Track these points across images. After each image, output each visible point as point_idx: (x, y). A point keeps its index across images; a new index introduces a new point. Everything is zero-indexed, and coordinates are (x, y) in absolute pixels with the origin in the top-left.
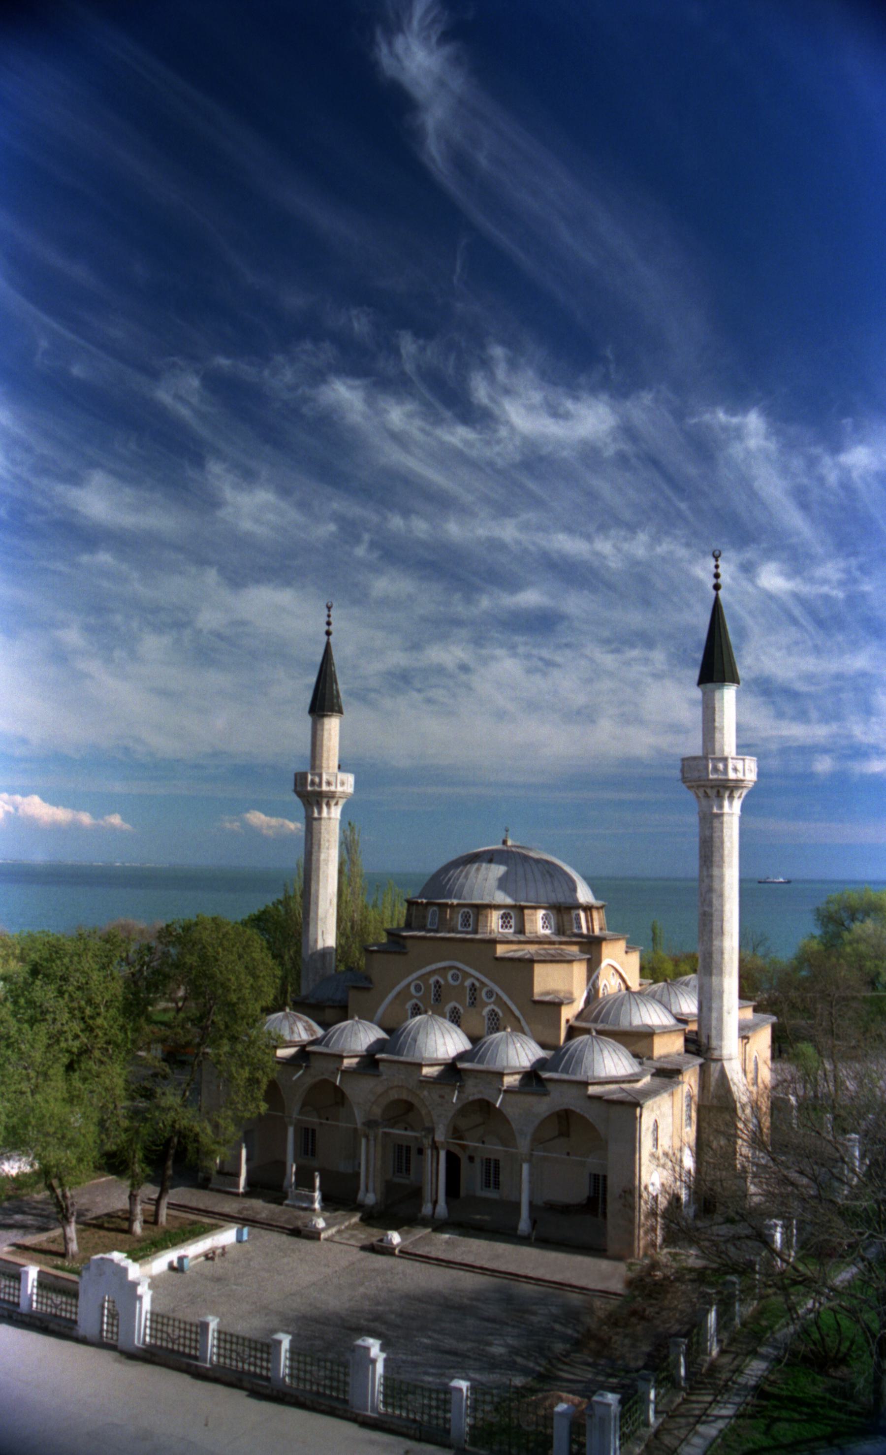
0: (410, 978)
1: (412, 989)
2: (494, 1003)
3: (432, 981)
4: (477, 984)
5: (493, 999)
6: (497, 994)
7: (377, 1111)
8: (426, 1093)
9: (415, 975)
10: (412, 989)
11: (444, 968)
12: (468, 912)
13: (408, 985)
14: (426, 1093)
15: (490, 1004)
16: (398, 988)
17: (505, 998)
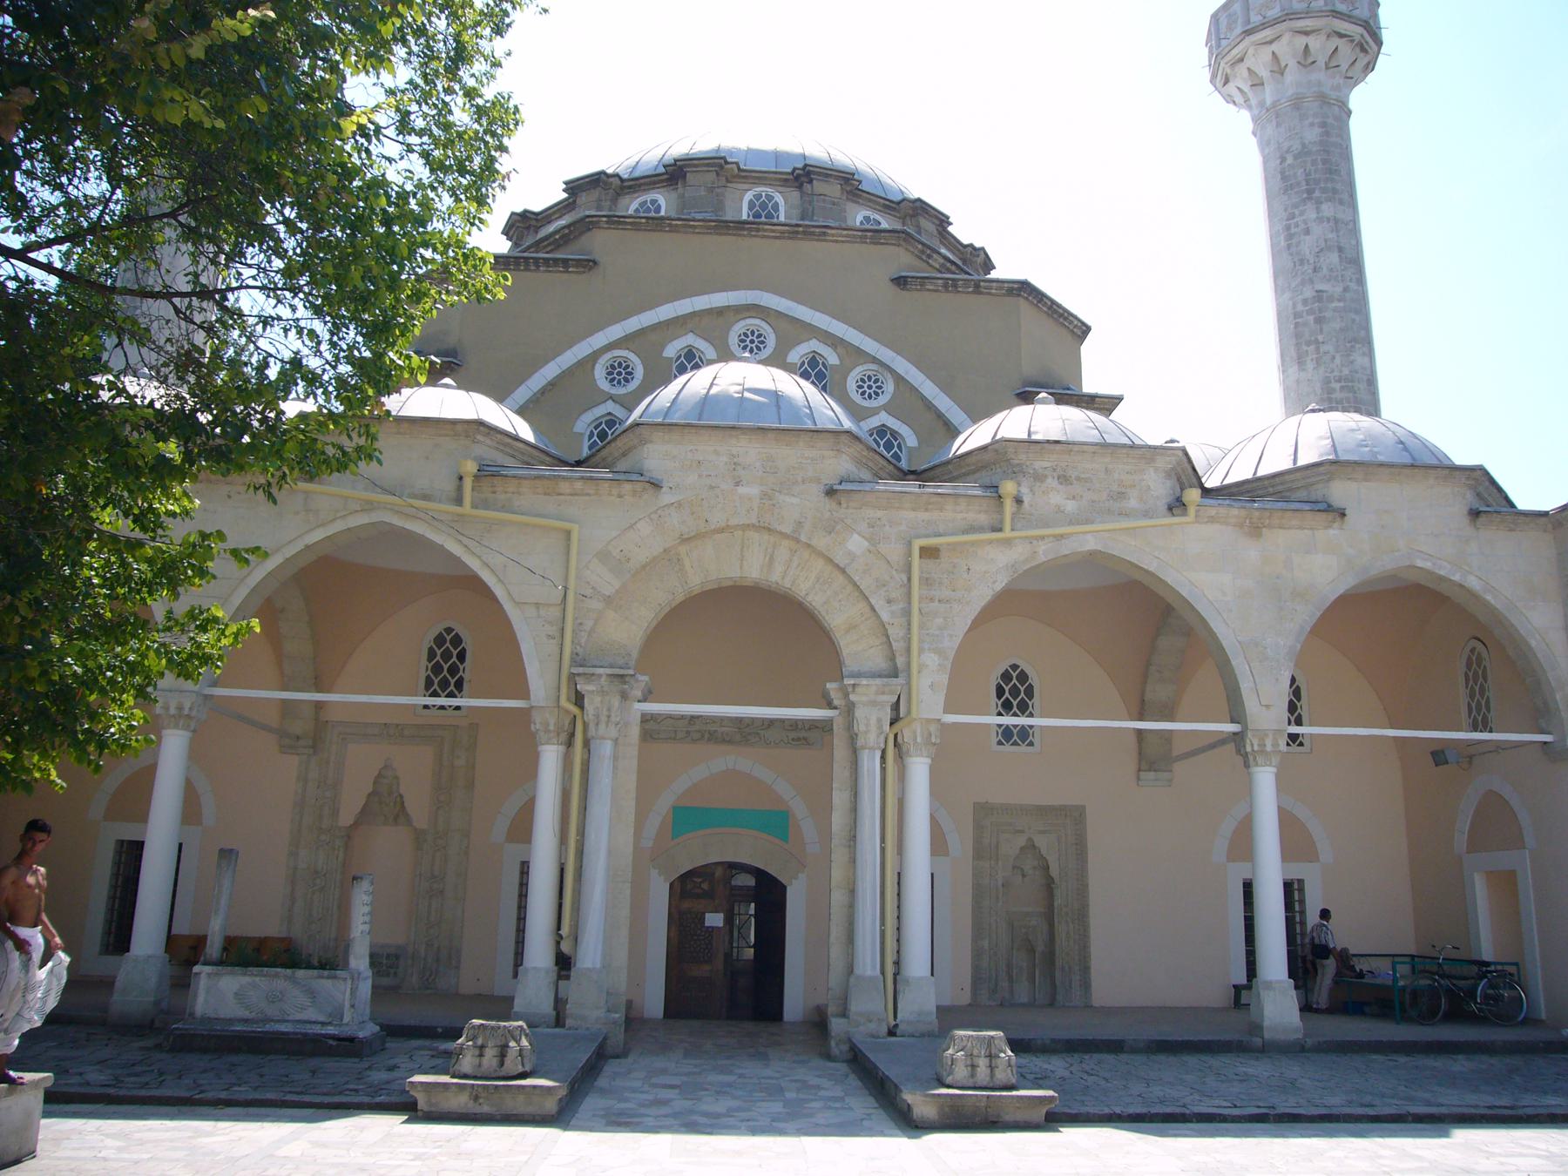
0: (599, 340)
1: (600, 372)
2: (886, 408)
3: (672, 350)
4: (832, 358)
5: (883, 399)
6: (899, 379)
7: (625, 631)
8: (856, 543)
9: (616, 331)
10: (600, 372)
11: (720, 312)
12: (770, 198)
13: (595, 356)
14: (856, 543)
15: (874, 412)
16: (550, 371)
17: (929, 389)
